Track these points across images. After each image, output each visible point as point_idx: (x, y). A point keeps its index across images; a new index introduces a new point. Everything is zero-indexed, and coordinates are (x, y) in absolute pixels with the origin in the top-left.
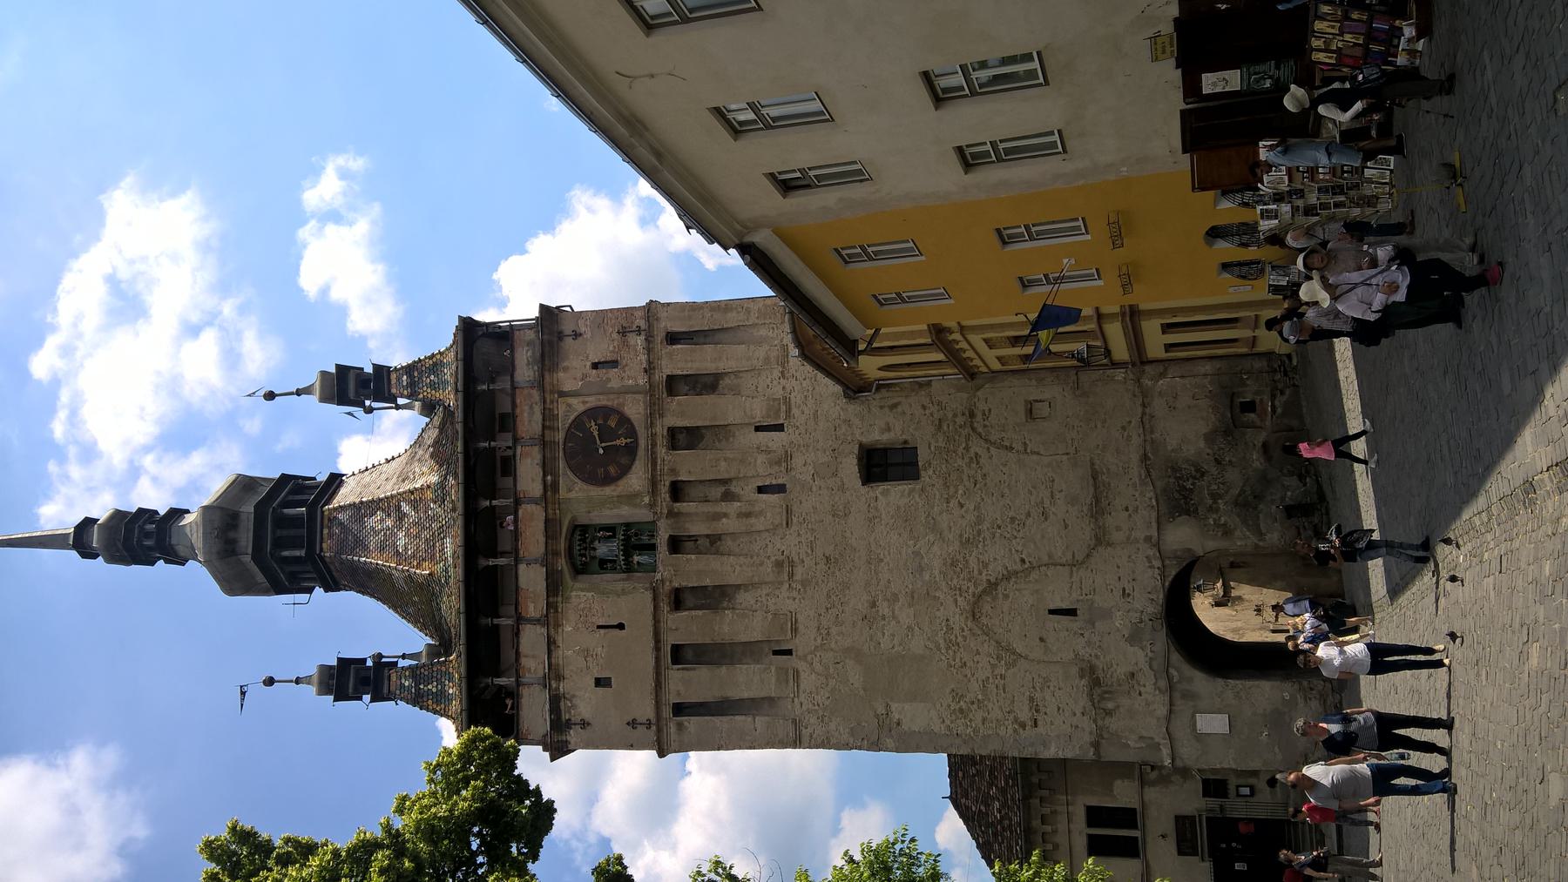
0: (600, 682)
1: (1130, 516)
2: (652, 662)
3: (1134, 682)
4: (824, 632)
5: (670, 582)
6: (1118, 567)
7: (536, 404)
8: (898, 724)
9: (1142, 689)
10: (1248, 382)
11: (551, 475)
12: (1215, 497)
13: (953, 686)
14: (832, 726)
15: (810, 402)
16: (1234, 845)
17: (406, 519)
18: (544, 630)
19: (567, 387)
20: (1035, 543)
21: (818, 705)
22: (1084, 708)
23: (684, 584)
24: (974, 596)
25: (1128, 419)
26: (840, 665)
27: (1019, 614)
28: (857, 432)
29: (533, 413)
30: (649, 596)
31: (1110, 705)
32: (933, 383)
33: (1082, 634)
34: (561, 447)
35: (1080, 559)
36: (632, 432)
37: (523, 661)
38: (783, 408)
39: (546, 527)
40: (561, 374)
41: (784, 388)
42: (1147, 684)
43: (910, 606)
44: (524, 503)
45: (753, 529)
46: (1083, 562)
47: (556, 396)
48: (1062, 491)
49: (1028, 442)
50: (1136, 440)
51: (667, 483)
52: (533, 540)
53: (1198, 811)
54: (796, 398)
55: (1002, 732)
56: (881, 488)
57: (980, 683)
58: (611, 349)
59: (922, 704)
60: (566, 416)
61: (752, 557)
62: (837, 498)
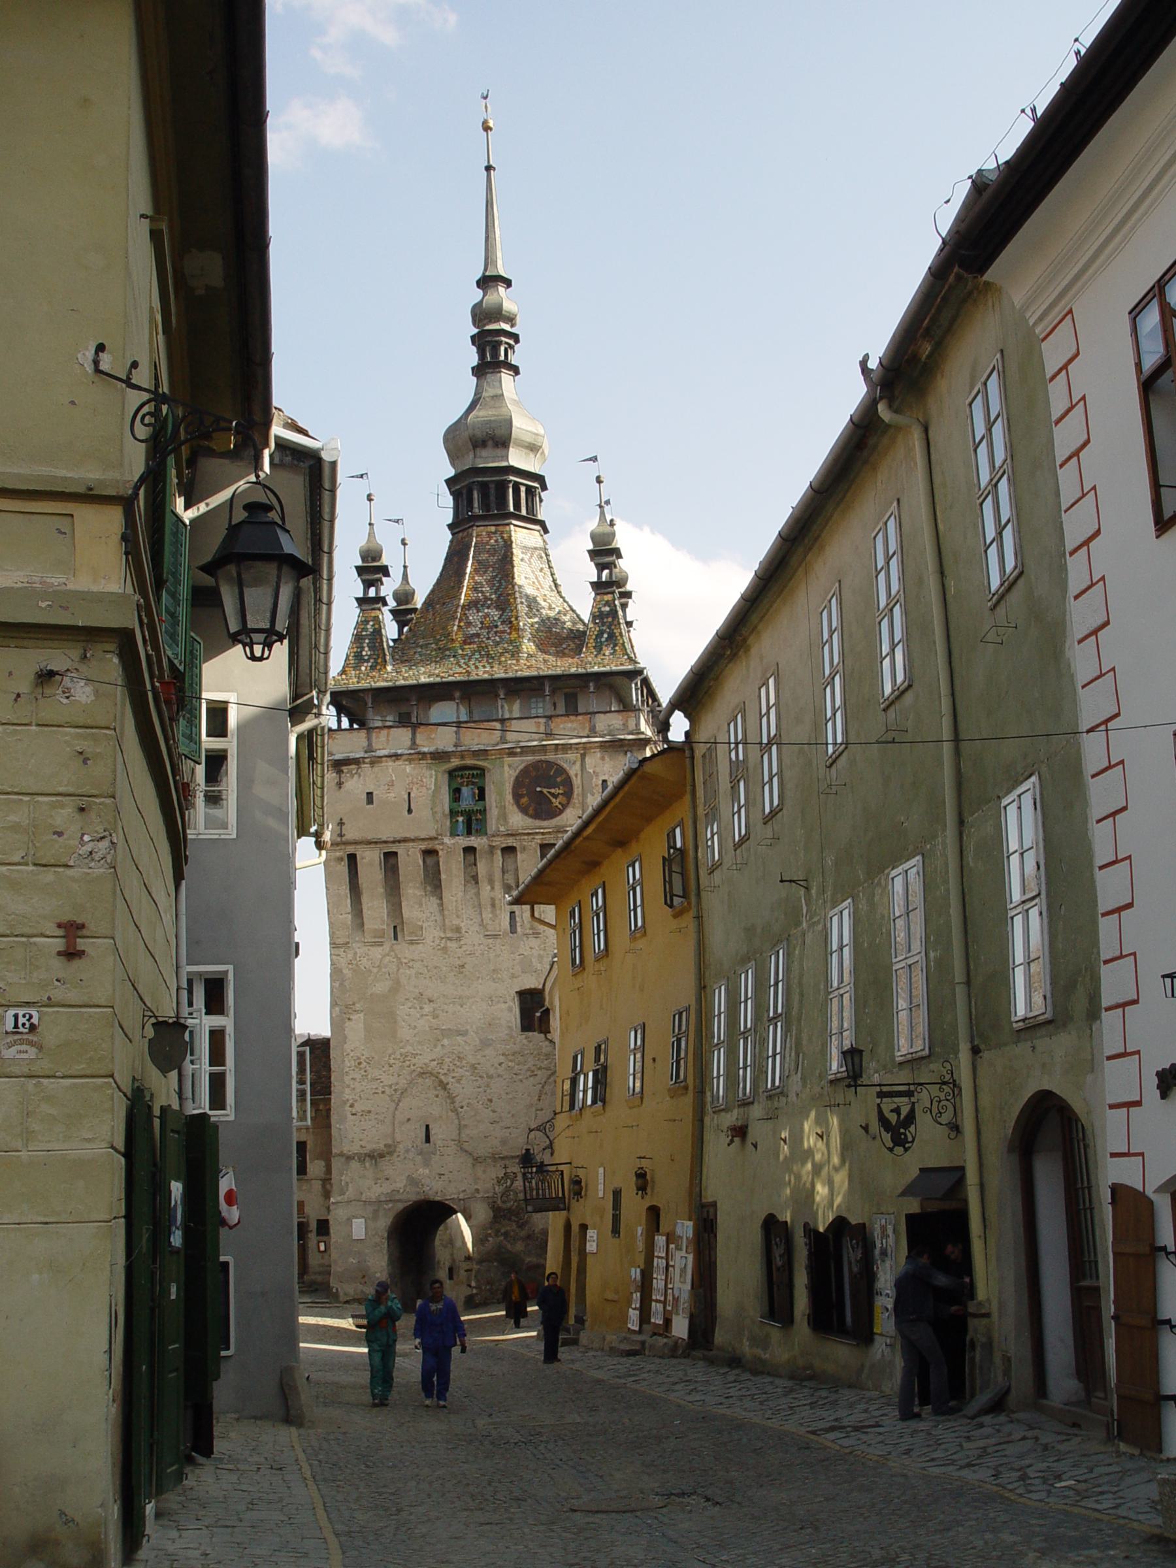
0: (370, 795)
2: (384, 839)
4: (411, 964)
8: (349, 1019)
12: (506, 1234)
13: (376, 1058)
19: (588, 760)
30: (433, 834)
31: (367, 1164)
34: (543, 758)
37: (385, 732)
40: (599, 755)
46: (461, 1148)
52: (476, 739)
53: (308, 1216)
55: (347, 1091)
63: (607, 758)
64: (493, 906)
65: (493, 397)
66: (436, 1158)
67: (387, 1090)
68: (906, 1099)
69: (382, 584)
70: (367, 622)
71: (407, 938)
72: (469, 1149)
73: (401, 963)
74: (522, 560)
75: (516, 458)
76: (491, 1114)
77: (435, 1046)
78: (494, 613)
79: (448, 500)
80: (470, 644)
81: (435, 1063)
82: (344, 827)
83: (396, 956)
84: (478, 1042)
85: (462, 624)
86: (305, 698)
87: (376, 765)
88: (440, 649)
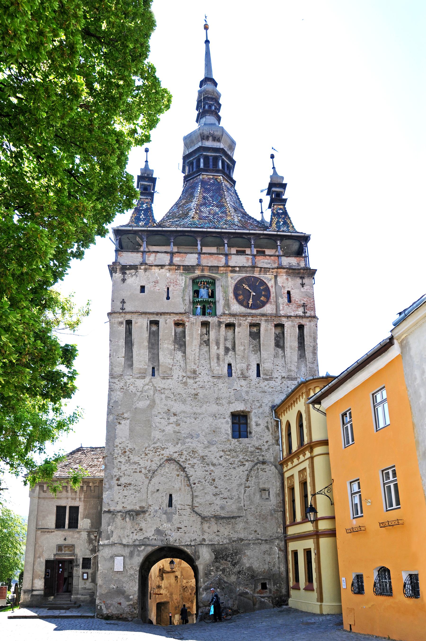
0: (143, 289)
1: (215, 533)
3: (138, 530)
4: (162, 391)
9: (135, 534)
10: (275, 586)
11: (239, 270)
12: (223, 570)
13: (136, 449)
14: (119, 393)
15: (270, 390)
16: (61, 570)
18: (167, 264)
20: (203, 489)
22: (126, 508)
23: (187, 328)
24: (179, 461)
25: (260, 533)
26: (147, 398)
28: (256, 411)
30: (183, 311)
31: (128, 519)
32: (278, 446)
33: (160, 508)
34: (252, 275)
37: (153, 255)
38: (268, 377)
39: (215, 266)
40: (285, 277)
41: (277, 378)
42: (137, 536)
43: (175, 432)
46: (194, 511)
47: (275, 274)
48: (227, 503)
49: (250, 488)
50: (250, 537)
51: (234, 322)
54: (272, 383)
55: (116, 470)
56: (230, 421)
57: (138, 462)
58: (297, 300)
59: (128, 435)
61: (198, 359)
63: (289, 279)
64: (218, 358)
66: (176, 517)
67: (143, 471)
72: (199, 512)
73: (156, 390)
76: (214, 488)
77: (177, 443)
82: (124, 304)
83: (153, 385)
84: (206, 442)
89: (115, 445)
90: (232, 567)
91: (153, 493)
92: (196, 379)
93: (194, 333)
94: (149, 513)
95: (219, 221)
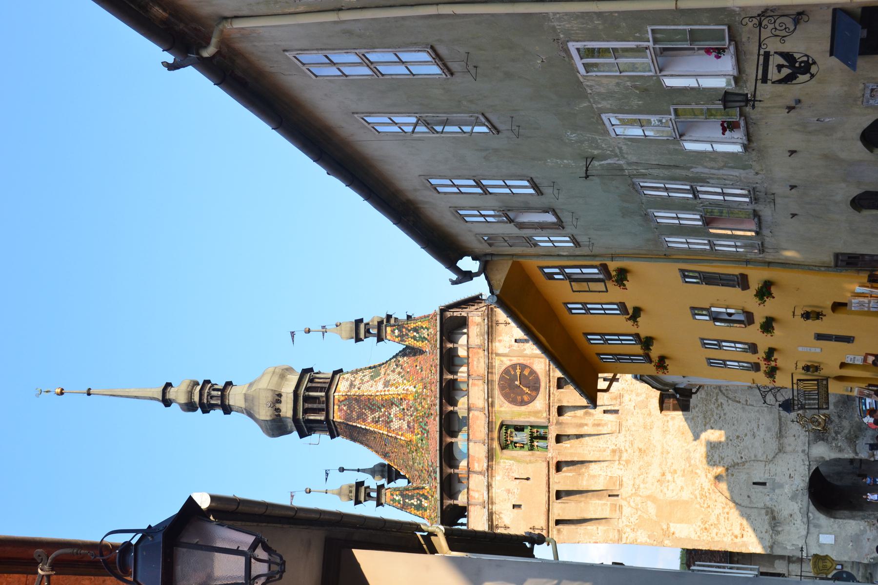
1: (796, 439)
4: (636, 486)
5: (556, 458)
6: (788, 464)
7: (481, 357)
8: (673, 534)
9: (795, 522)
11: (491, 398)
12: (837, 433)
13: (702, 516)
14: (639, 533)
17: (394, 408)
19: (500, 351)
20: (748, 449)
21: (632, 523)
22: (767, 529)
23: (563, 460)
26: (644, 504)
27: (738, 484)
29: (480, 362)
30: (545, 465)
31: (780, 529)
33: (768, 495)
34: (497, 383)
35: (770, 459)
36: (537, 380)
37: (471, 493)
42: (798, 520)
43: (683, 476)
44: (473, 410)
45: (601, 433)
46: (772, 460)
47: (494, 355)
48: (763, 425)
49: (748, 400)
51: (557, 407)
55: (725, 539)
59: (686, 525)
60: (500, 366)
62: (646, 420)
63: (499, 338)
65: (245, 402)
66: (777, 479)
67: (726, 510)
68: (771, 58)
69: (368, 487)
70: (394, 500)
71: (618, 488)
72: (772, 455)
73: (635, 493)
74: (359, 389)
75: (288, 389)
77: (696, 473)
78: (394, 410)
79: (315, 437)
80: (414, 429)
81: (708, 474)
82: (536, 528)
83: (629, 497)
85: (400, 433)
86: (423, 542)
87: (494, 500)
88: (416, 450)
89: (698, 539)
90: (833, 424)
91: (751, 502)
92: (621, 450)
93: (570, 451)
94: (773, 506)
95: (417, 410)
